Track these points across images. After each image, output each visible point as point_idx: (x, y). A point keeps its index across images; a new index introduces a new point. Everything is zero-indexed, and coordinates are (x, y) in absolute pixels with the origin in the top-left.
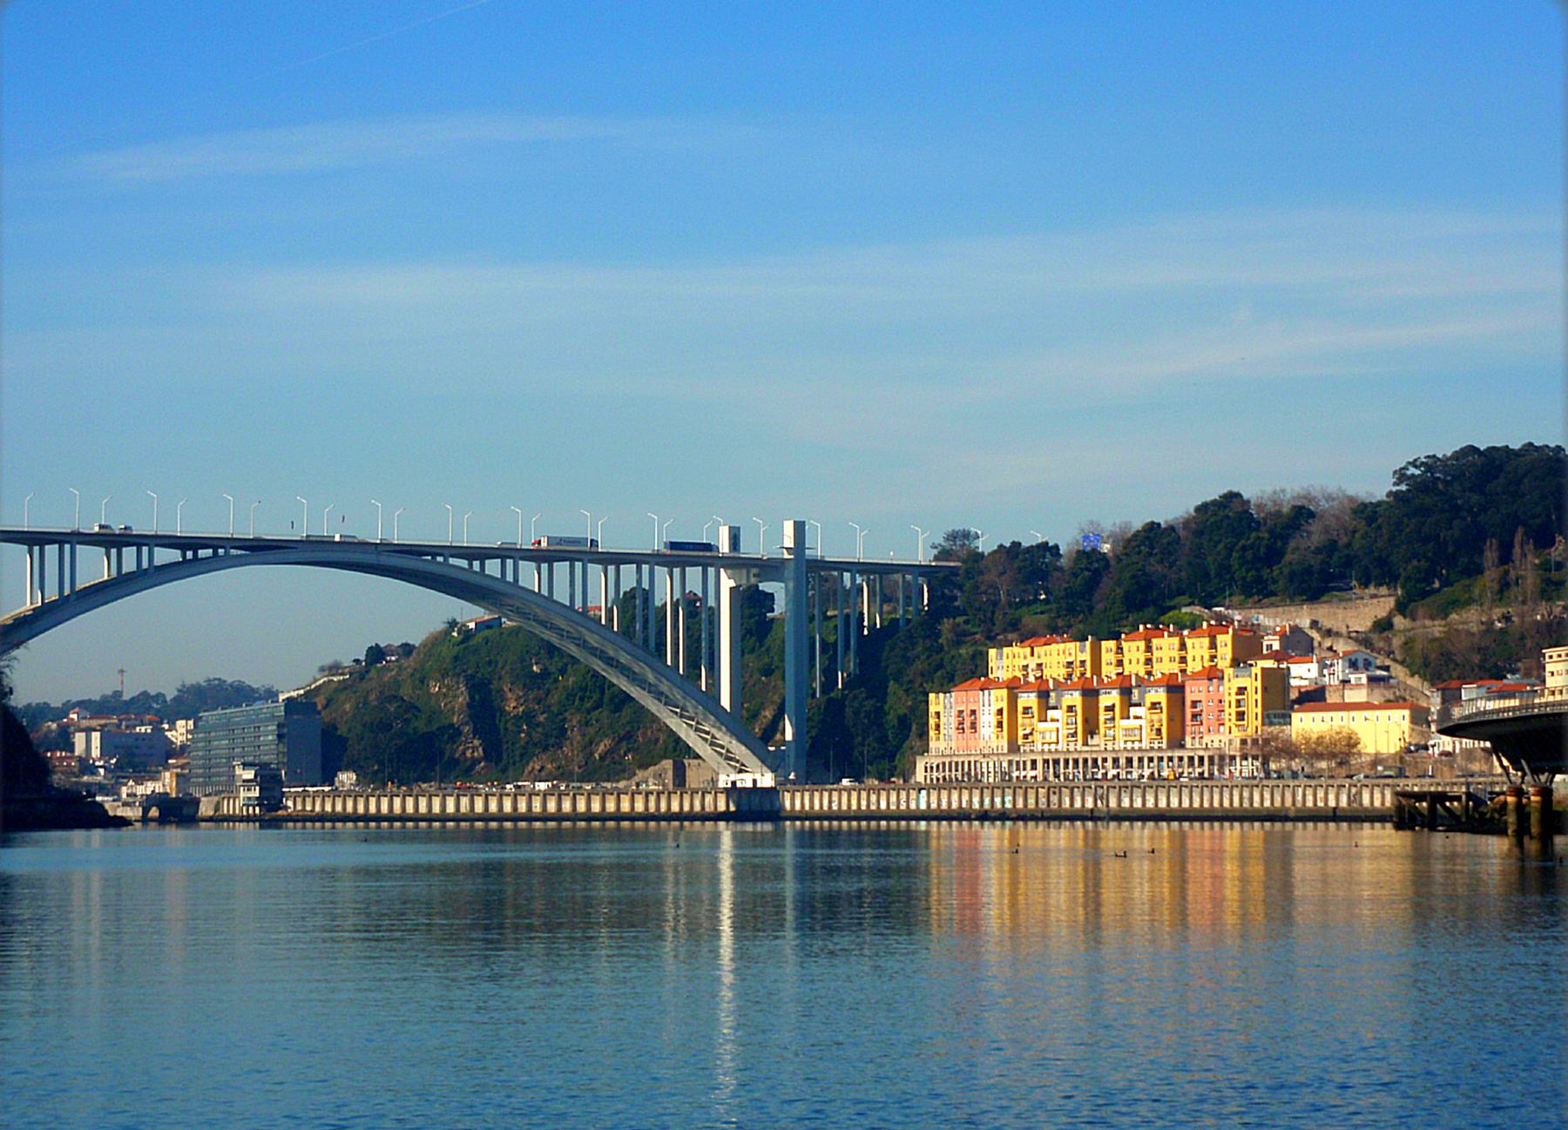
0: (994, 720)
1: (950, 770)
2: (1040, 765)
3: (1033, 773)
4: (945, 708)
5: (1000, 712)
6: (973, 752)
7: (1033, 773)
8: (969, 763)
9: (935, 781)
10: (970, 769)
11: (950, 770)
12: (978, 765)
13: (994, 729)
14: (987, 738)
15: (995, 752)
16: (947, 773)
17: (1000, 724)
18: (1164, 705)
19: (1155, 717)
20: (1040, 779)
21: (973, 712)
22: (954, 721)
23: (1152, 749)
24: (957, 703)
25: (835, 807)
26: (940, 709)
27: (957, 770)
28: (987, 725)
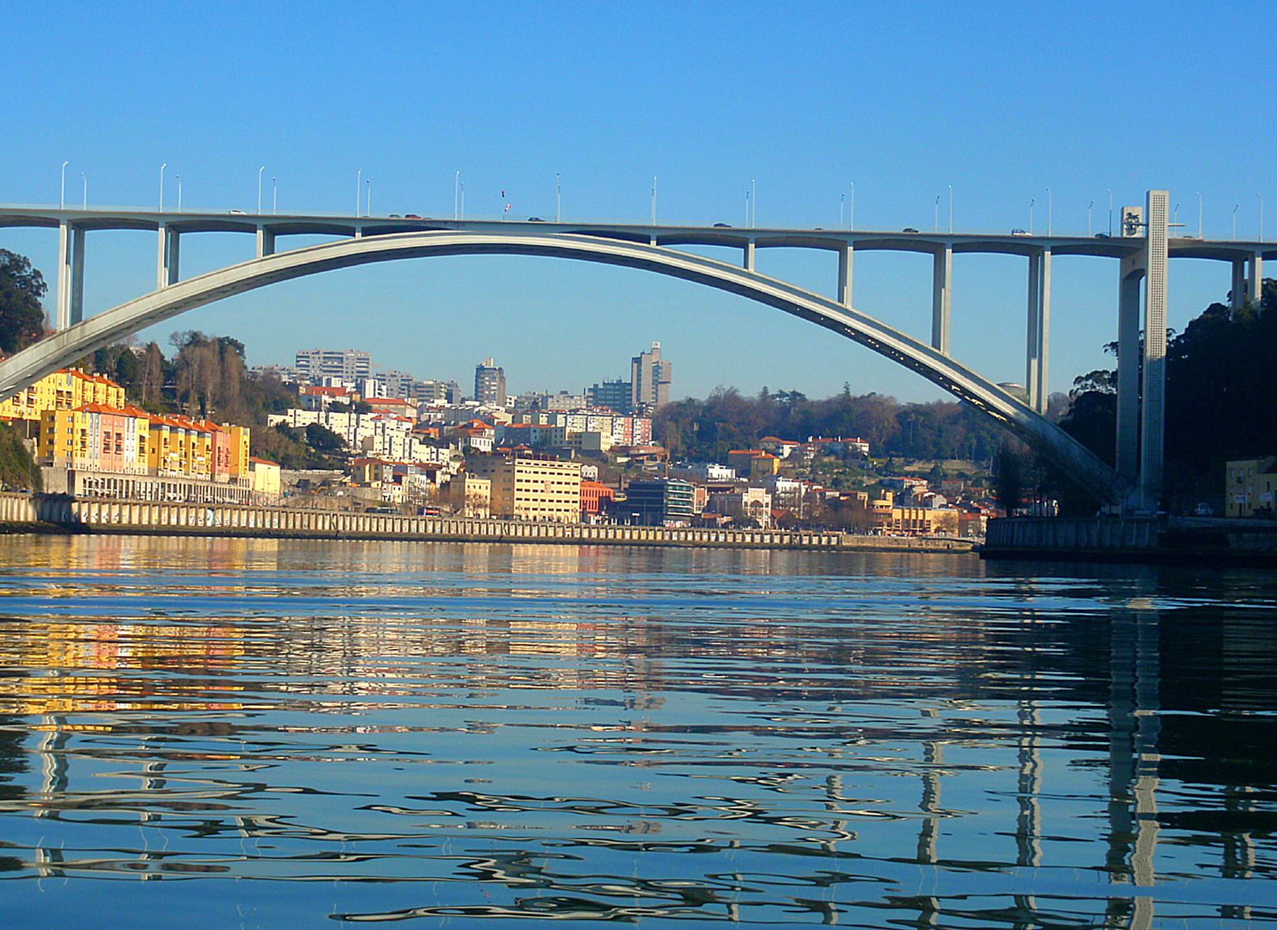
0: (136, 443)
1: (109, 487)
4: (91, 427)
5: (142, 438)
6: (117, 472)
8: (127, 481)
10: (127, 488)
11: (109, 487)
12: (131, 484)
14: (130, 460)
15: (137, 473)
16: (112, 490)
17: (142, 449)
21: (119, 435)
22: (100, 439)
24: (103, 424)
25: (374, 529)
26: (86, 427)
27: (115, 488)
28: (130, 449)
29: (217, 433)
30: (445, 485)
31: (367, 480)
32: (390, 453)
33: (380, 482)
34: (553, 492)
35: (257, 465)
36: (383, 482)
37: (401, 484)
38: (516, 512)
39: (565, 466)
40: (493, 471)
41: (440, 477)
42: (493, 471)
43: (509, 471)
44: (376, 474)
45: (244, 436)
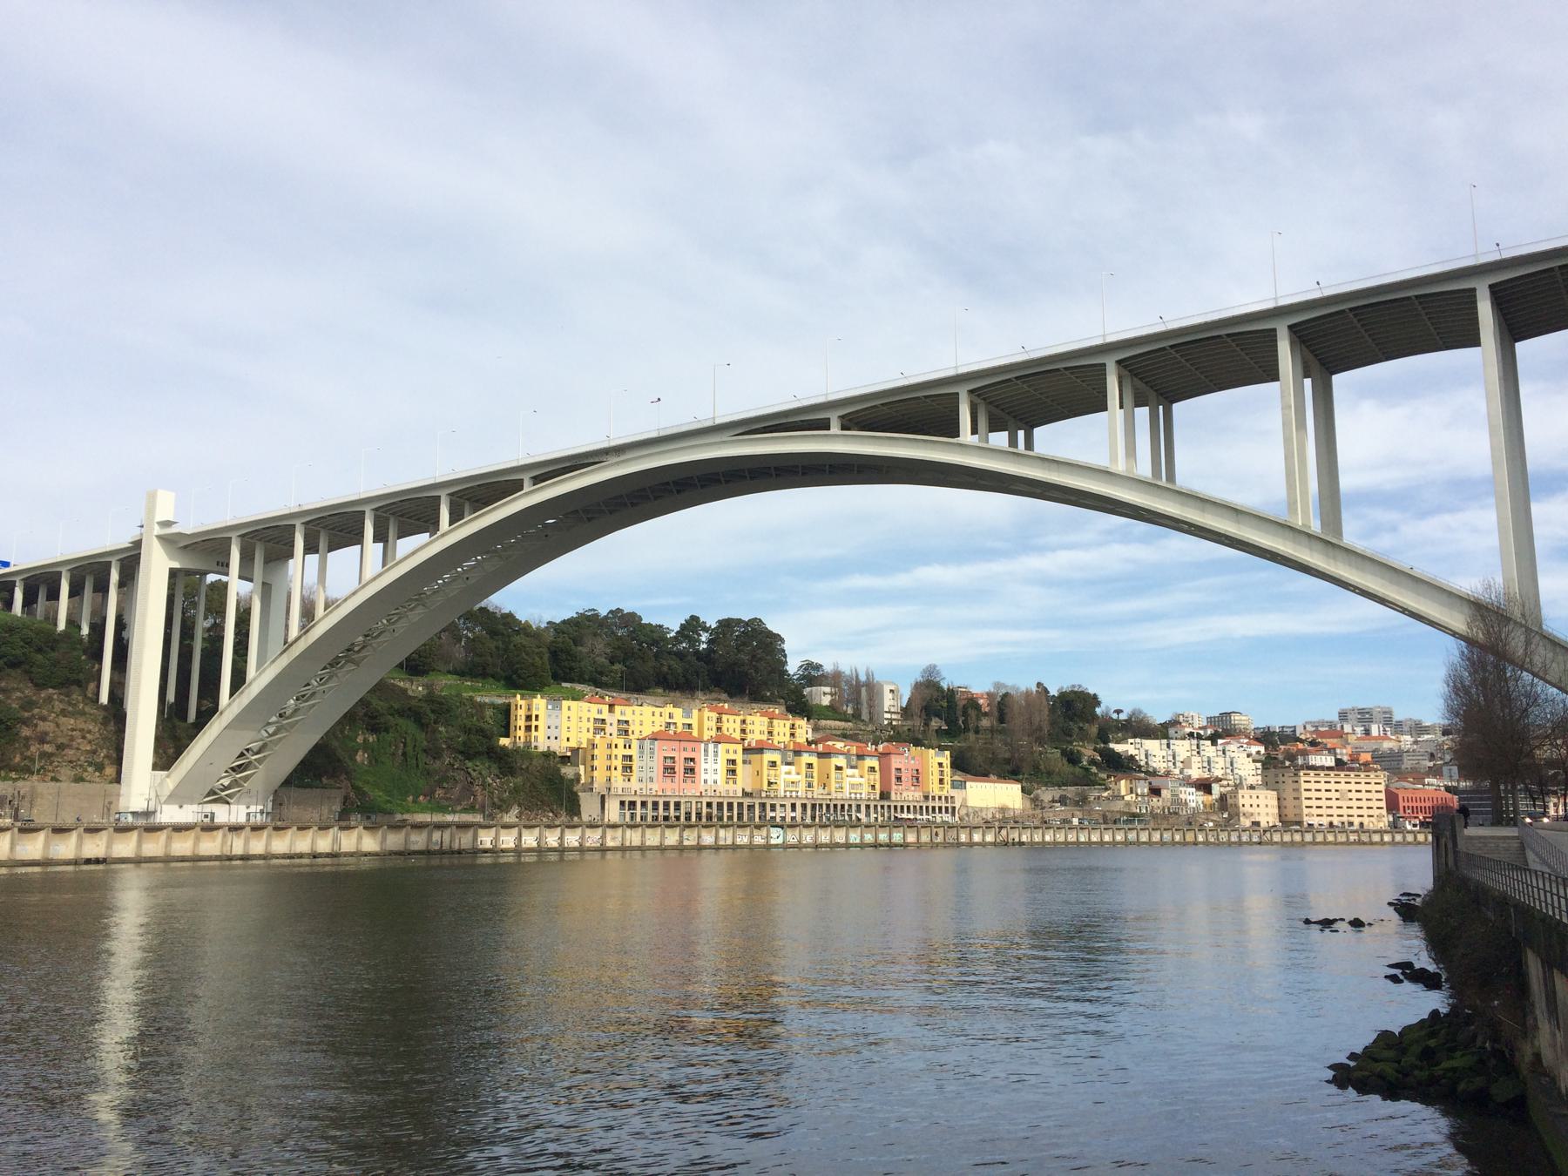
0: (722, 766)
2: (799, 808)
3: (793, 814)
7: (793, 814)
9: (893, 819)
13: (721, 775)
18: (877, 768)
19: (872, 777)
20: (799, 819)
23: (869, 799)
29: (893, 757)
30: (1223, 798)
31: (1123, 793)
32: (1209, 770)
33: (1134, 795)
34: (1351, 799)
35: (968, 784)
36: (1137, 795)
37: (1160, 796)
38: (1305, 819)
39: (1342, 775)
40: (1284, 782)
41: (1217, 789)
42: (1284, 782)
43: (1297, 782)
44: (1131, 789)
45: (946, 758)
